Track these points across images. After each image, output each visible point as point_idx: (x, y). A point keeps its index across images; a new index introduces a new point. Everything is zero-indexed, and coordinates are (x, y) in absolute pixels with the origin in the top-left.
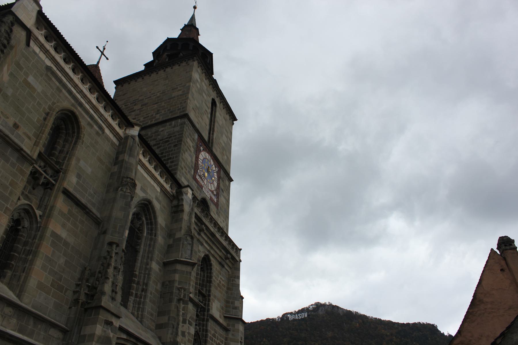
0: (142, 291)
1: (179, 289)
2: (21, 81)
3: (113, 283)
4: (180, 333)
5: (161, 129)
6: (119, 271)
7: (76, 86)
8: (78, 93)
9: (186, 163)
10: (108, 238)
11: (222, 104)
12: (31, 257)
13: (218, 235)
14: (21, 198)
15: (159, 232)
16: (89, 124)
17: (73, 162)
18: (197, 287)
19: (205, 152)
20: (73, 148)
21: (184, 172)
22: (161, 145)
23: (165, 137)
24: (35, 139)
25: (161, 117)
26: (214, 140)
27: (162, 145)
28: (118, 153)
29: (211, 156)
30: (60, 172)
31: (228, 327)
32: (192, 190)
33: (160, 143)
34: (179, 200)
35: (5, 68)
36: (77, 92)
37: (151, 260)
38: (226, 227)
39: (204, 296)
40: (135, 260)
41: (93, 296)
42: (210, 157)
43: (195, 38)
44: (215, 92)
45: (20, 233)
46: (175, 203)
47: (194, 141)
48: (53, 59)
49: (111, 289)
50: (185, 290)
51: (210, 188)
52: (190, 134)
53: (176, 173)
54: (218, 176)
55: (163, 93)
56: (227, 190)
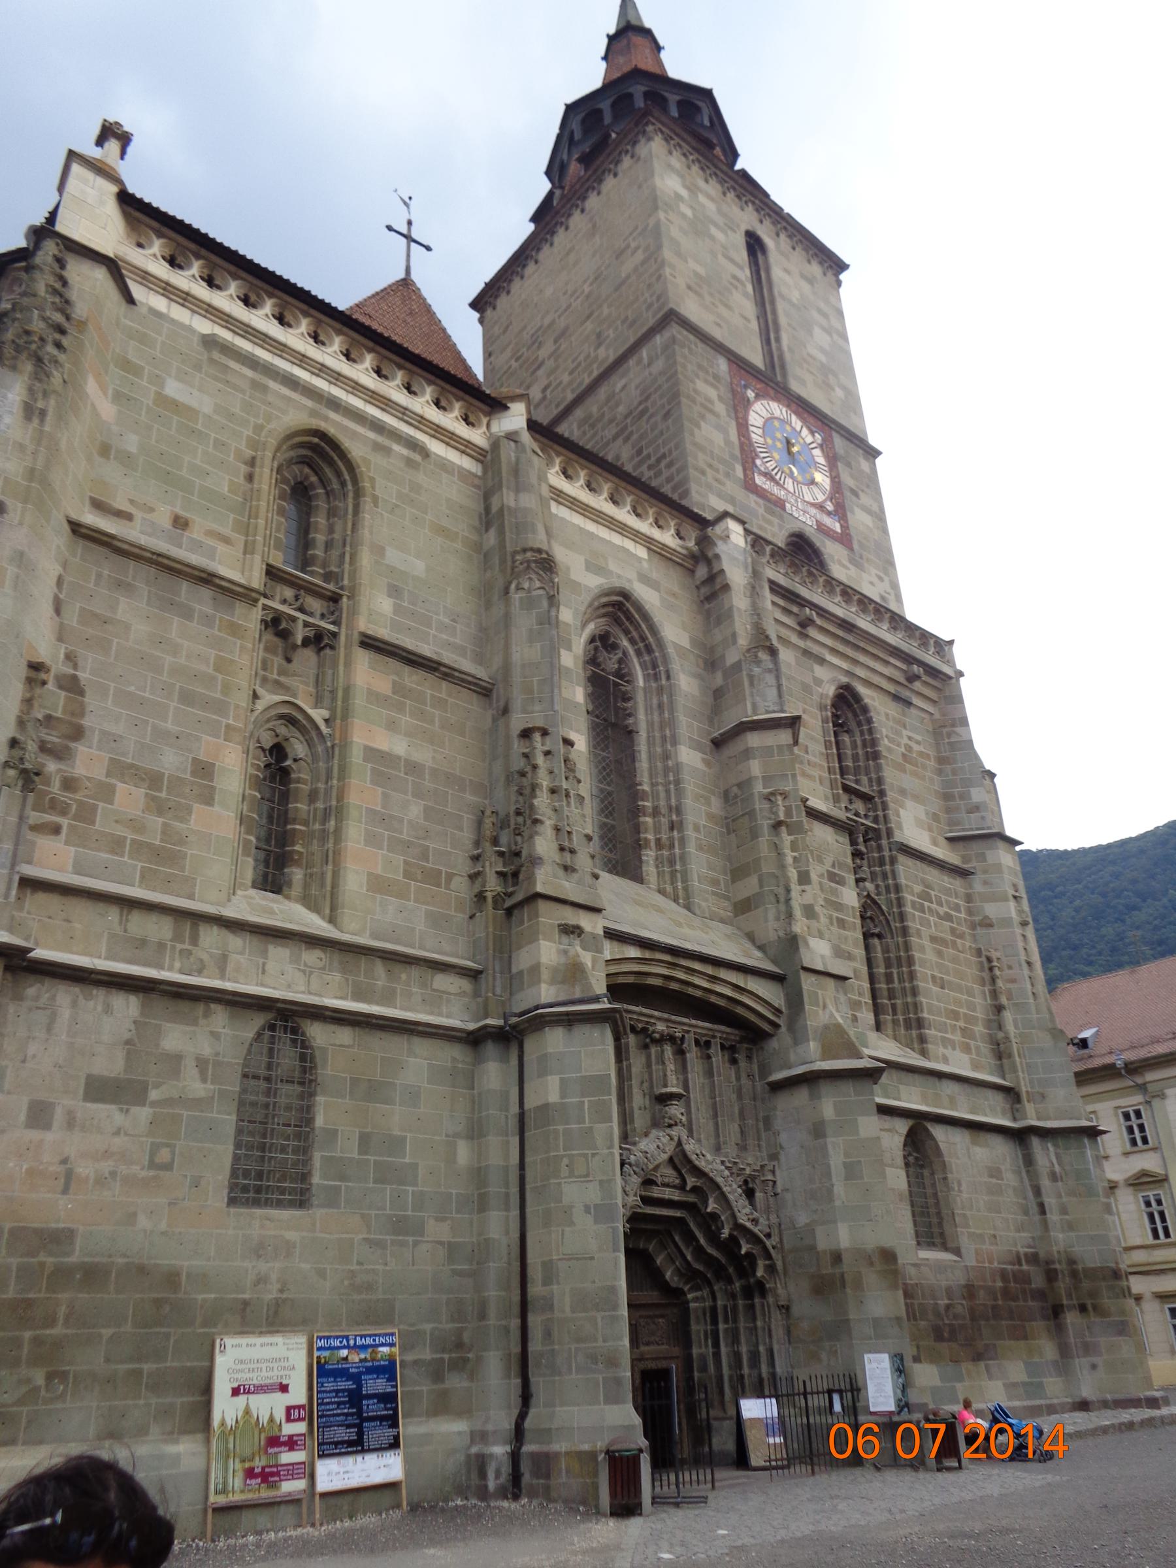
0: (672, 828)
1: (769, 798)
2: (150, 403)
3: (557, 829)
4: (798, 912)
5: (619, 386)
6: (567, 795)
7: (302, 360)
8: (318, 375)
9: (712, 452)
10: (518, 721)
11: (783, 236)
12: (333, 823)
13: (863, 623)
14: (261, 691)
15: (676, 665)
16: (377, 447)
17: (366, 559)
18: (836, 779)
19: (765, 402)
20: (354, 525)
21: (710, 480)
22: (630, 429)
23: (636, 403)
24: (243, 538)
25: (611, 352)
26: (787, 356)
27: (634, 428)
28: (487, 496)
29: (788, 406)
30: (341, 596)
31: (965, 866)
32: (742, 522)
33: (626, 427)
34: (709, 562)
35: (91, 386)
36: (313, 373)
37: (675, 743)
38: (892, 592)
39: (866, 798)
40: (633, 758)
41: (515, 875)
42: (784, 410)
43: (647, 65)
44: (750, 207)
45: (293, 776)
46: (702, 572)
47: (719, 382)
48: (211, 312)
49: (554, 846)
50: (785, 796)
51: (808, 498)
52: (700, 367)
53: (686, 493)
54: (827, 457)
55: (596, 279)
56: (868, 486)
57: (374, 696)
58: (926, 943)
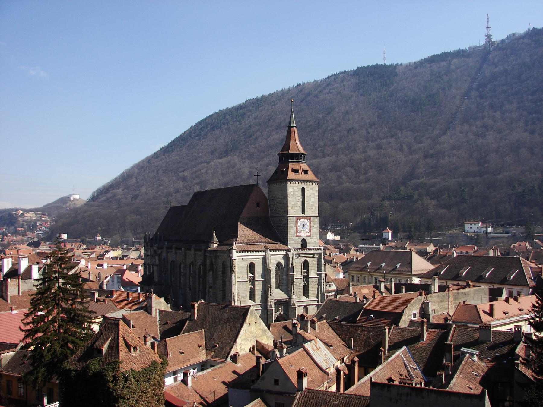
17: (256, 272)
51: (305, 232)
57: (257, 285)
58: (311, 287)
